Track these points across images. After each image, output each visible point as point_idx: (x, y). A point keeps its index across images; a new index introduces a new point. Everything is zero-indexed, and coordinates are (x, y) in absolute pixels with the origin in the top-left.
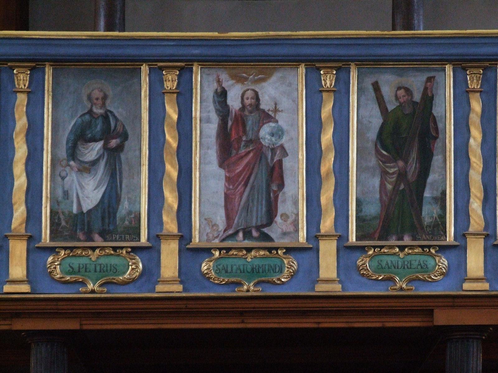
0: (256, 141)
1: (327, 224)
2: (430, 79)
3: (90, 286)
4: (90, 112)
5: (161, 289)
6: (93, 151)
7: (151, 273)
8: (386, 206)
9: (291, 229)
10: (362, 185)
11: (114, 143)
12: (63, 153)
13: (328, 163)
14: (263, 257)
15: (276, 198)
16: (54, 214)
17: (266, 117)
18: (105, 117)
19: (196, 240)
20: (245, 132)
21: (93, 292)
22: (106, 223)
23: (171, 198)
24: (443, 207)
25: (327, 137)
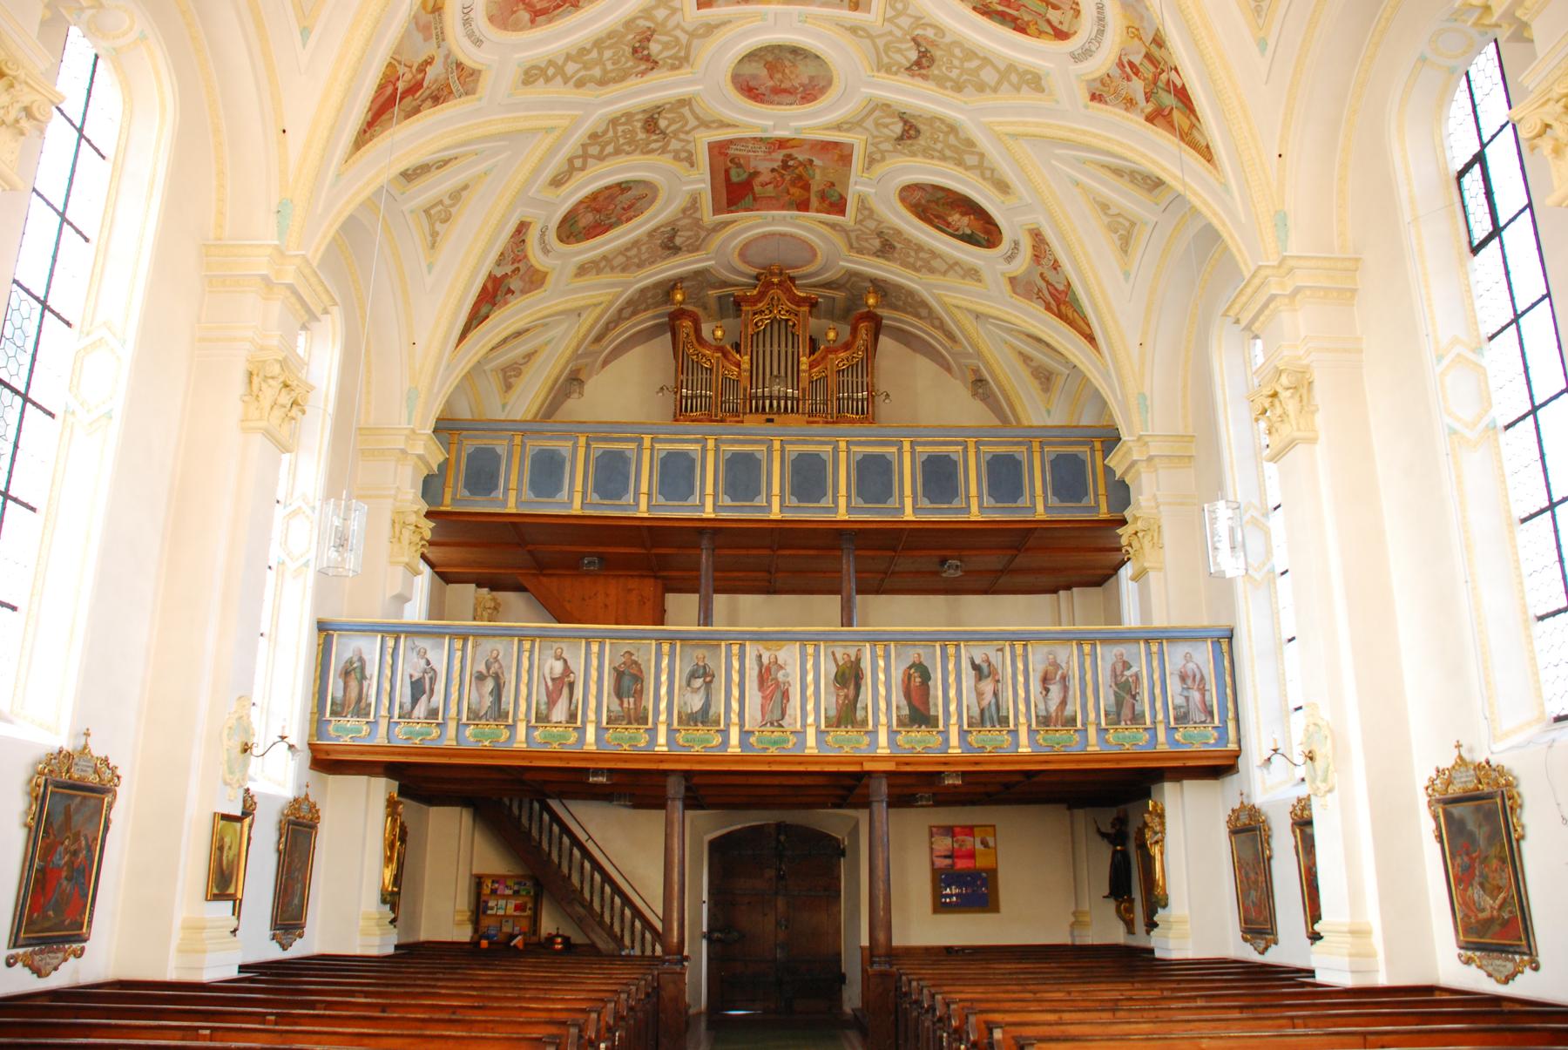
0: (776, 679)
1: (810, 720)
5: (731, 751)
6: (698, 682)
7: (725, 743)
8: (839, 711)
10: (829, 700)
13: (810, 691)
17: (781, 667)
19: (747, 728)
22: (703, 717)
23: (735, 706)
25: (810, 678)
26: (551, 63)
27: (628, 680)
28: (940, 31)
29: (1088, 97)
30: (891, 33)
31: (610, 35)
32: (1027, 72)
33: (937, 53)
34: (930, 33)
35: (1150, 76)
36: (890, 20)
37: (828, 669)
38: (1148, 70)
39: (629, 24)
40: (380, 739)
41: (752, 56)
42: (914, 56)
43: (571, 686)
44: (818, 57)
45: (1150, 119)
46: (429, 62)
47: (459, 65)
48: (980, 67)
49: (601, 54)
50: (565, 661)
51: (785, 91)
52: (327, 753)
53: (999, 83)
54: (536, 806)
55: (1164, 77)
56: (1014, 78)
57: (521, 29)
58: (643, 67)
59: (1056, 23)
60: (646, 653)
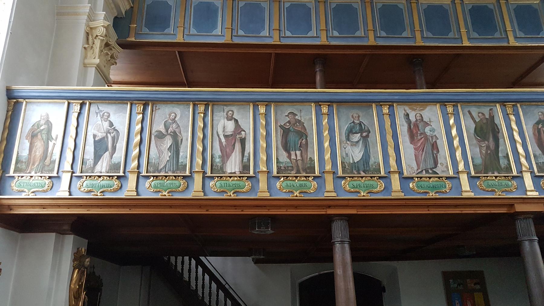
0: (424, 133)
1: (461, 167)
2: (491, 110)
3: (362, 194)
4: (353, 122)
6: (356, 137)
7: (388, 188)
9: (446, 169)
10: (474, 151)
11: (364, 134)
12: (344, 138)
14: (437, 181)
15: (437, 156)
16: (342, 163)
17: (427, 124)
18: (360, 124)
19: (406, 174)
20: (419, 130)
21: (364, 196)
22: (364, 167)
24: (509, 160)
27: (293, 137)
37: (467, 125)
40: (62, 191)
43: (243, 142)
50: (236, 121)
52: (10, 207)
54: (193, 262)
60: (309, 117)
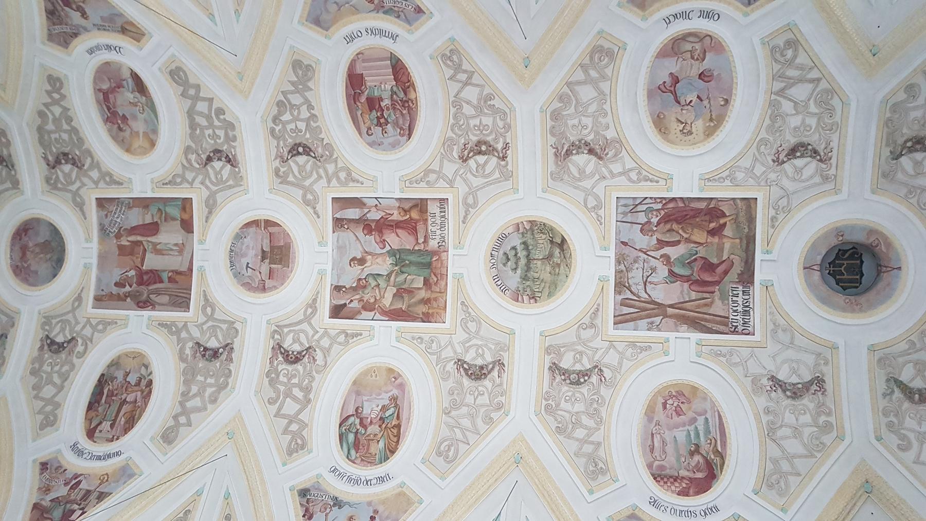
26: (63, 97)
28: (82, 355)
29: (43, 460)
30: (77, 323)
31: (81, 141)
32: (55, 417)
33: (63, 355)
34: (80, 348)
35: (72, 497)
36: (88, 321)
38: (77, 495)
39: (89, 153)
41: (55, 232)
42: (60, 339)
44: (55, 276)
45: (36, 506)
46: (84, 15)
47: (76, 35)
48: (54, 384)
49: (65, 131)
51: (24, 254)
53: (42, 399)
55: (76, 507)
56: (49, 408)
57: (95, 82)
58: (50, 158)
59: (99, 428)
